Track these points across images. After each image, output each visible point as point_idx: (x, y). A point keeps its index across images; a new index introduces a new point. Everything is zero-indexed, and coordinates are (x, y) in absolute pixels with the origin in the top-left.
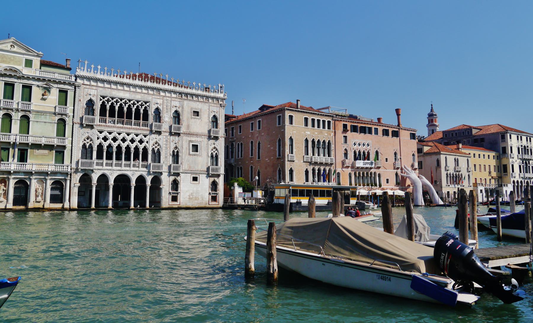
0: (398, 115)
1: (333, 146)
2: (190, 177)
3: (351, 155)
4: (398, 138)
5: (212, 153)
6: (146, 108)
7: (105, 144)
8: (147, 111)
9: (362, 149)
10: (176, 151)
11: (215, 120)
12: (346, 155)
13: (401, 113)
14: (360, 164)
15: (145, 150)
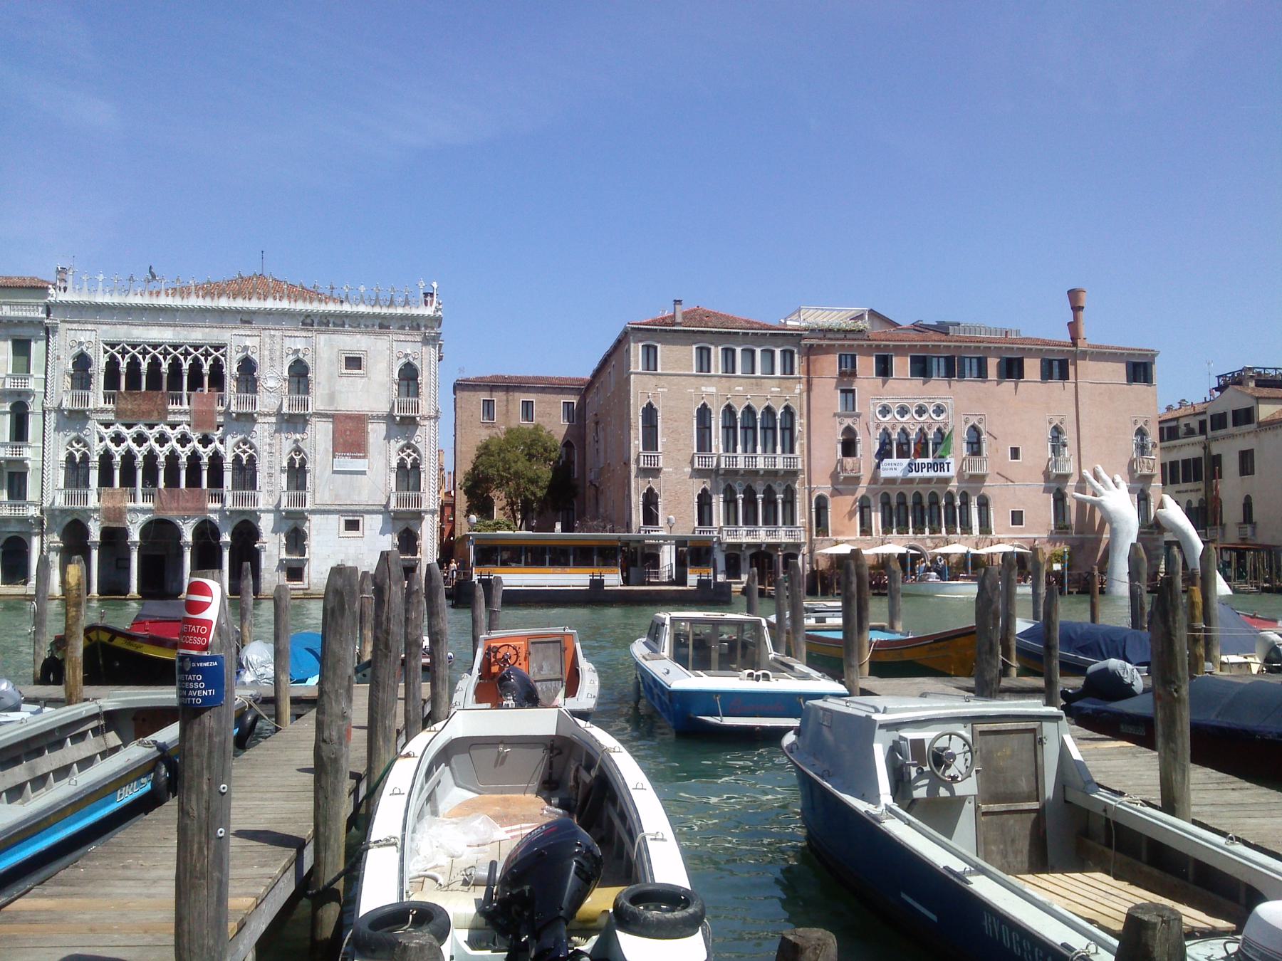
0: (1076, 309)
1: (799, 425)
2: (337, 522)
3: (868, 445)
4: (1070, 385)
5: (402, 459)
6: (216, 360)
7: (118, 452)
8: (222, 367)
9: (912, 424)
10: (297, 458)
11: (409, 376)
12: (849, 447)
13: (1085, 301)
14: (895, 468)
15: (216, 459)
